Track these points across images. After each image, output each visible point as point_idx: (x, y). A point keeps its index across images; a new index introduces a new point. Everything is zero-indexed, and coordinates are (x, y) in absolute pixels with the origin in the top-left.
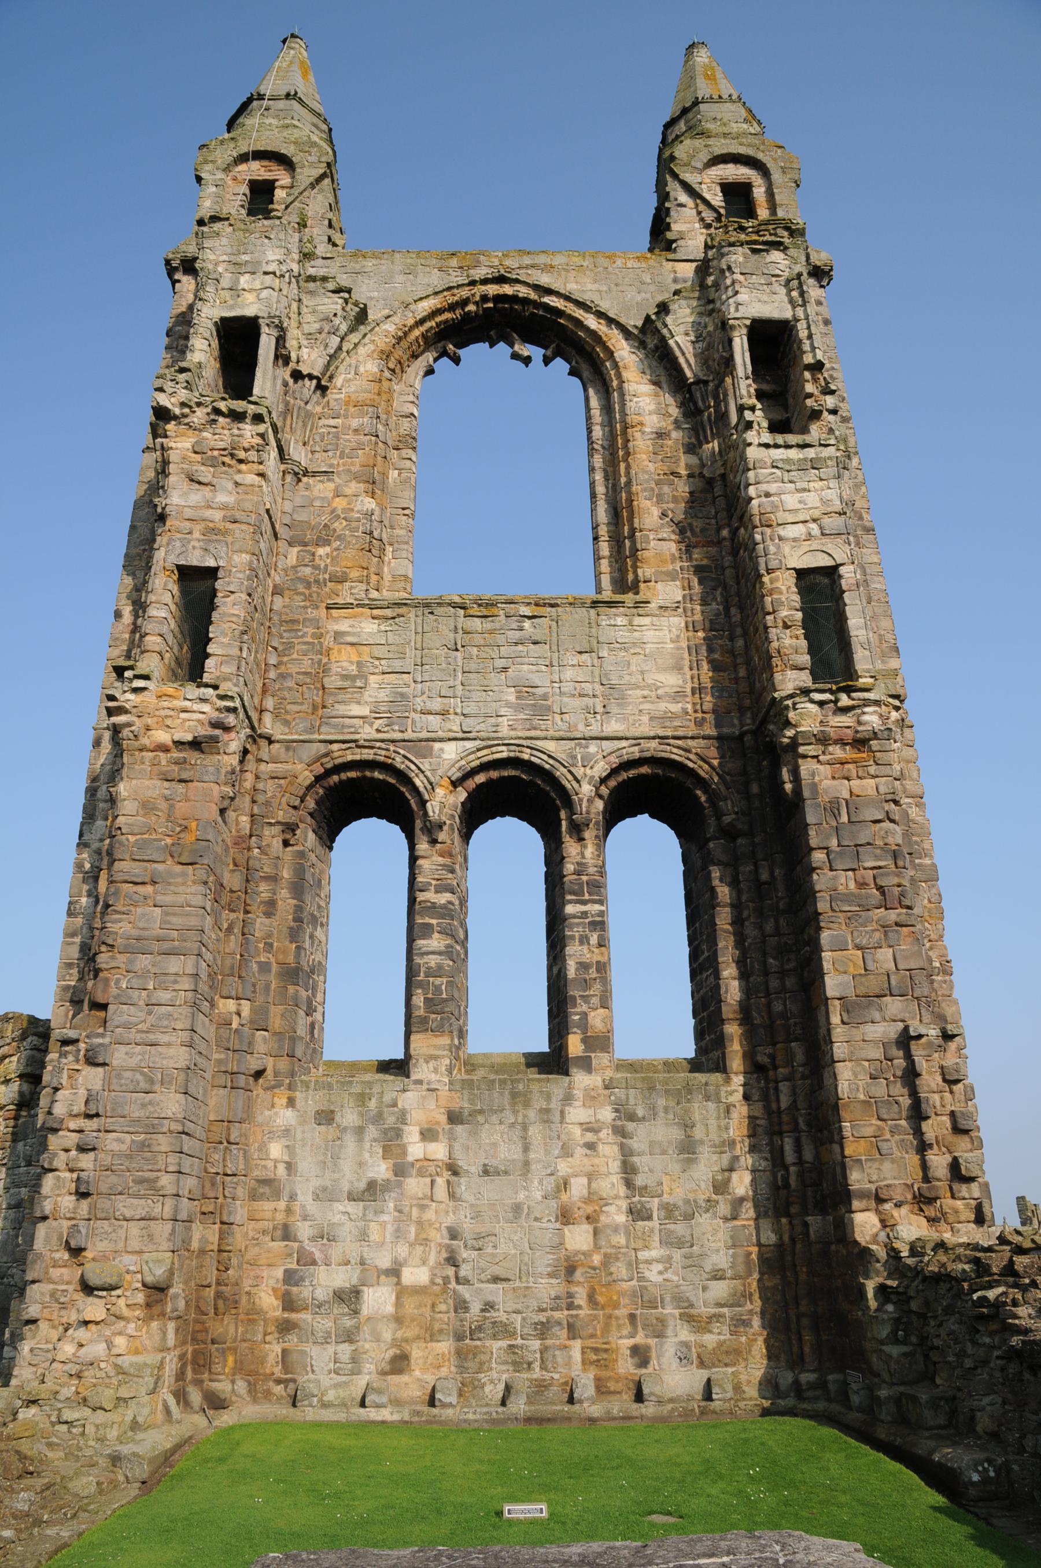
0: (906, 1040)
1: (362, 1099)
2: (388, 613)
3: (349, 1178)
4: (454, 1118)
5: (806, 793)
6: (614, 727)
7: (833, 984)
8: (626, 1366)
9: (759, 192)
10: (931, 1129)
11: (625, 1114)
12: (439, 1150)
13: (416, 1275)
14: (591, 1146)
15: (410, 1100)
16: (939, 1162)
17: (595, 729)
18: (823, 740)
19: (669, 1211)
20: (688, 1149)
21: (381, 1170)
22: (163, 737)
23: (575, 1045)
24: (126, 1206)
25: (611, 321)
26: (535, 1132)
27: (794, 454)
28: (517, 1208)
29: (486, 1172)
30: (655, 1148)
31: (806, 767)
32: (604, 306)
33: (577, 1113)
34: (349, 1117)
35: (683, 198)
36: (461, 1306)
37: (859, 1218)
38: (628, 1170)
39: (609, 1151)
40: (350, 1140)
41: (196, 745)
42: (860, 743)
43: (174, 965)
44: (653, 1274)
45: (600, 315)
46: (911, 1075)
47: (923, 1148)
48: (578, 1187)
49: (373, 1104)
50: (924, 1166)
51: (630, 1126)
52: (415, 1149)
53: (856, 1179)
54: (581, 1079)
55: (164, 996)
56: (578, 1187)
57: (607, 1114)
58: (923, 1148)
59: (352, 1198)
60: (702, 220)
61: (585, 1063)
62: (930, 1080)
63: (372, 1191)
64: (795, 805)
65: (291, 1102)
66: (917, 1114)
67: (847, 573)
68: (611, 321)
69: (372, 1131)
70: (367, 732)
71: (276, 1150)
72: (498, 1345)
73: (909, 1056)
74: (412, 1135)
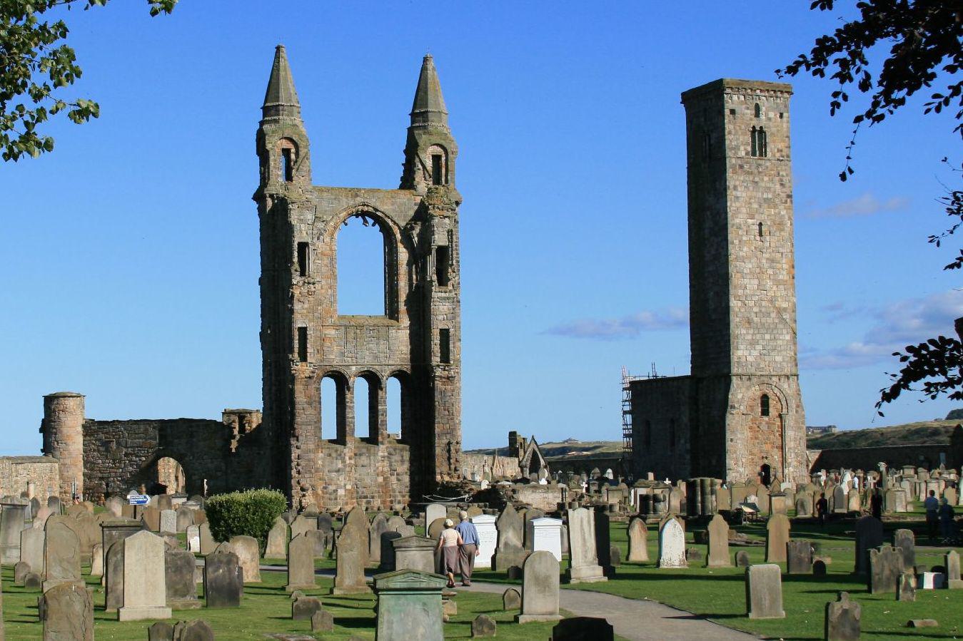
0: (449, 444)
1: (336, 451)
2: (337, 328)
3: (334, 467)
4: (355, 455)
5: (436, 388)
6: (391, 362)
7: (437, 430)
8: (388, 504)
9: (443, 159)
10: (451, 461)
11: (390, 454)
12: (353, 462)
13: (349, 487)
14: (383, 461)
15: (346, 450)
16: (453, 467)
17: (387, 363)
18: (441, 377)
19: (398, 474)
20: (402, 461)
21: (340, 465)
22: (303, 376)
23: (380, 439)
24: (307, 476)
25: (395, 223)
26: (372, 457)
27: (443, 295)
28: (368, 473)
29: (363, 466)
30: (396, 461)
31: (436, 382)
32: (395, 219)
33: (380, 454)
34: (334, 455)
35: (420, 166)
36: (358, 493)
37: (437, 476)
38: (391, 465)
39: (387, 463)
40: (335, 461)
41: (310, 377)
42: (448, 378)
43: (309, 427)
44: (394, 486)
45: (392, 221)
46: (449, 451)
47: (450, 464)
48: (380, 468)
49: (339, 452)
50: (450, 468)
51: (391, 456)
52: (348, 462)
53: (438, 470)
54: (381, 446)
55: (308, 434)
56: (380, 468)
57: (386, 454)
58: (450, 464)
59: (336, 472)
60: (424, 177)
61: (382, 443)
62: (453, 451)
63: (338, 471)
64: (433, 389)
65: (322, 452)
66: (449, 458)
67: (451, 330)
68: (395, 223)
69: (339, 458)
70: (335, 363)
71: (320, 462)
72: (365, 500)
73: (449, 447)
74: (347, 458)
